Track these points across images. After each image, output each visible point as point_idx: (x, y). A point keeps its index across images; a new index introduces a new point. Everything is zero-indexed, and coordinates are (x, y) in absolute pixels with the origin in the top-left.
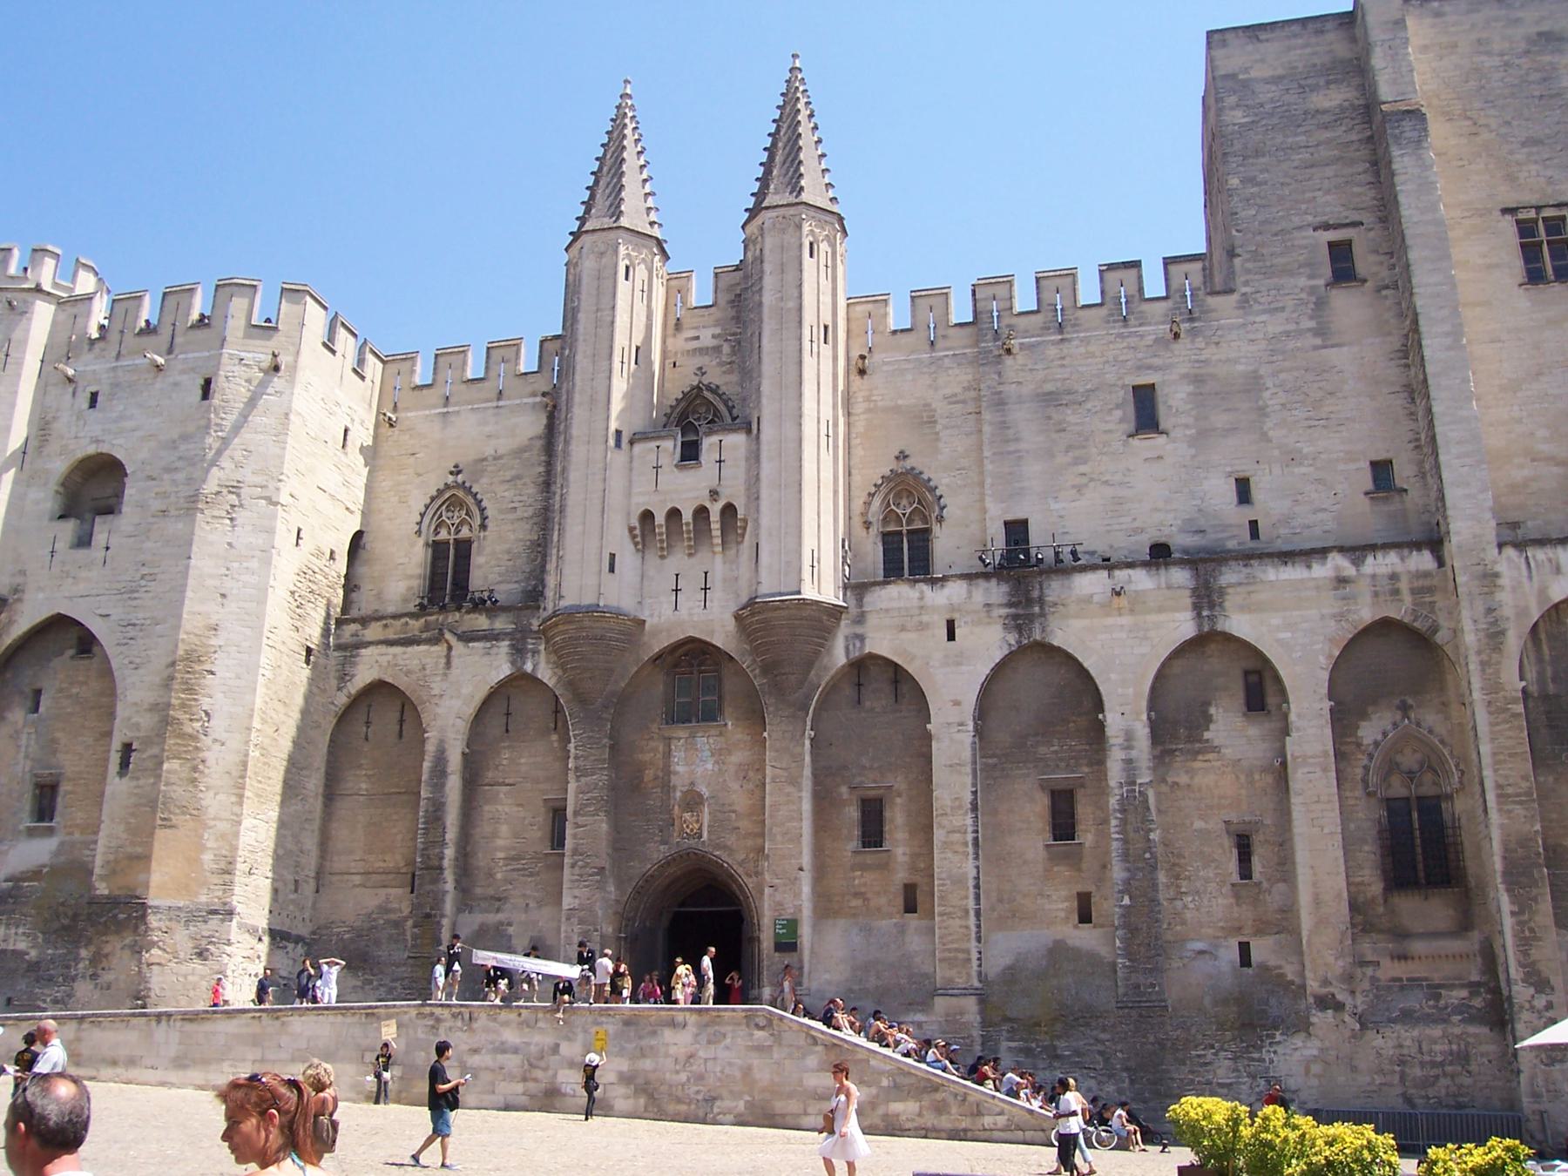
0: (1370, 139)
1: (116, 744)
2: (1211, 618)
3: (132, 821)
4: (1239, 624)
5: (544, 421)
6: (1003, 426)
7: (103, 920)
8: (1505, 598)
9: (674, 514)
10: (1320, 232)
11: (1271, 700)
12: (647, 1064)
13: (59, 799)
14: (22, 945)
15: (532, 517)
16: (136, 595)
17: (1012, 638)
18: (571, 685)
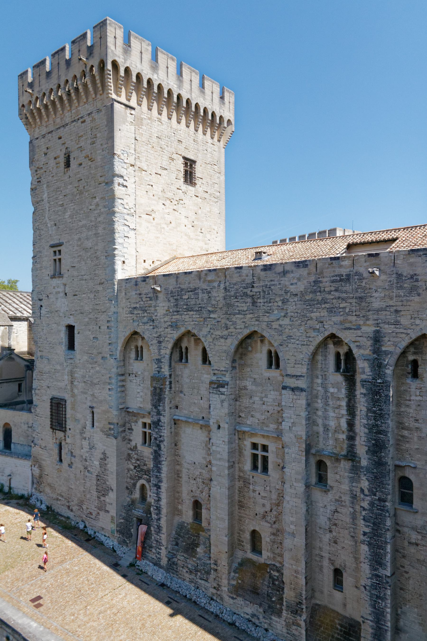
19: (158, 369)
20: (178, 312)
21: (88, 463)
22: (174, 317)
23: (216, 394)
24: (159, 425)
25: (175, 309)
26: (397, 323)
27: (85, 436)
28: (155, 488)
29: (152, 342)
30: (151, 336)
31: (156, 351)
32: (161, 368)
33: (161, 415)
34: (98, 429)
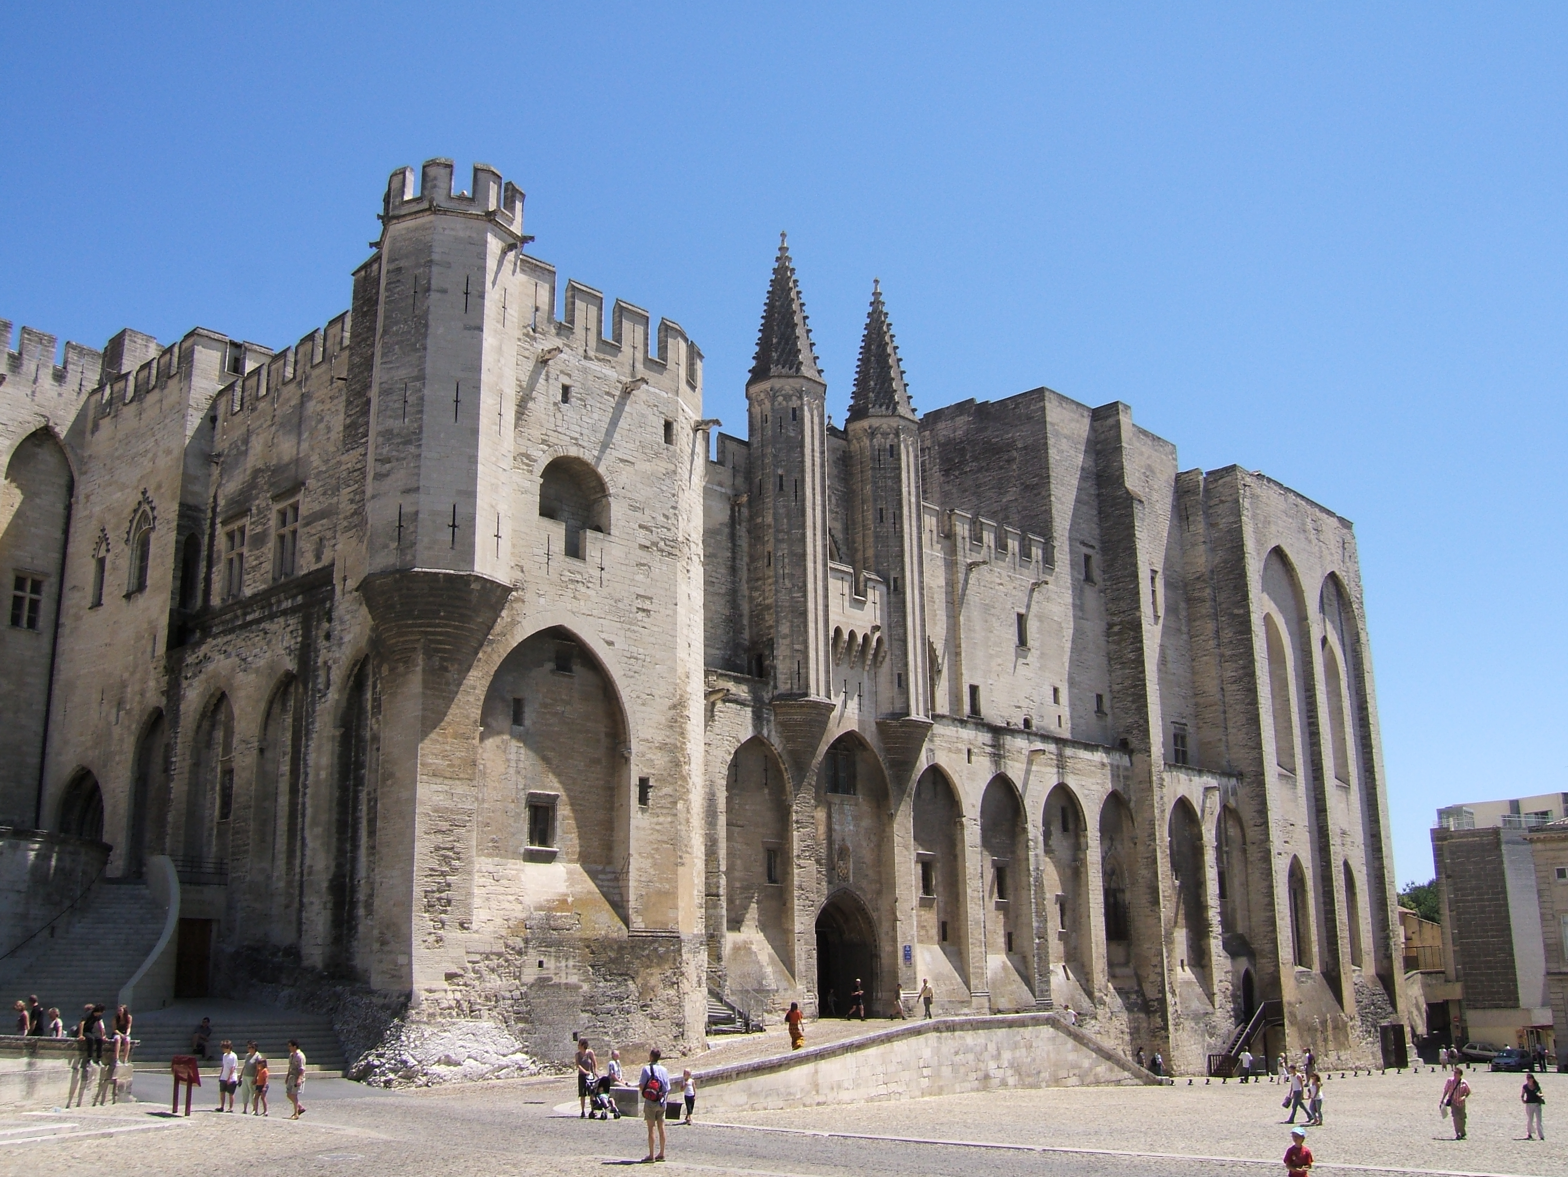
0: (1098, 495)
1: (634, 781)
2: (1063, 774)
3: (657, 856)
4: (1072, 783)
5: (729, 512)
6: (969, 619)
7: (647, 952)
8: (1164, 790)
9: (852, 634)
10: (1081, 547)
11: (1071, 826)
12: (1017, 1053)
13: (558, 824)
14: (574, 979)
15: (724, 595)
16: (633, 628)
17: (993, 768)
18: (791, 753)
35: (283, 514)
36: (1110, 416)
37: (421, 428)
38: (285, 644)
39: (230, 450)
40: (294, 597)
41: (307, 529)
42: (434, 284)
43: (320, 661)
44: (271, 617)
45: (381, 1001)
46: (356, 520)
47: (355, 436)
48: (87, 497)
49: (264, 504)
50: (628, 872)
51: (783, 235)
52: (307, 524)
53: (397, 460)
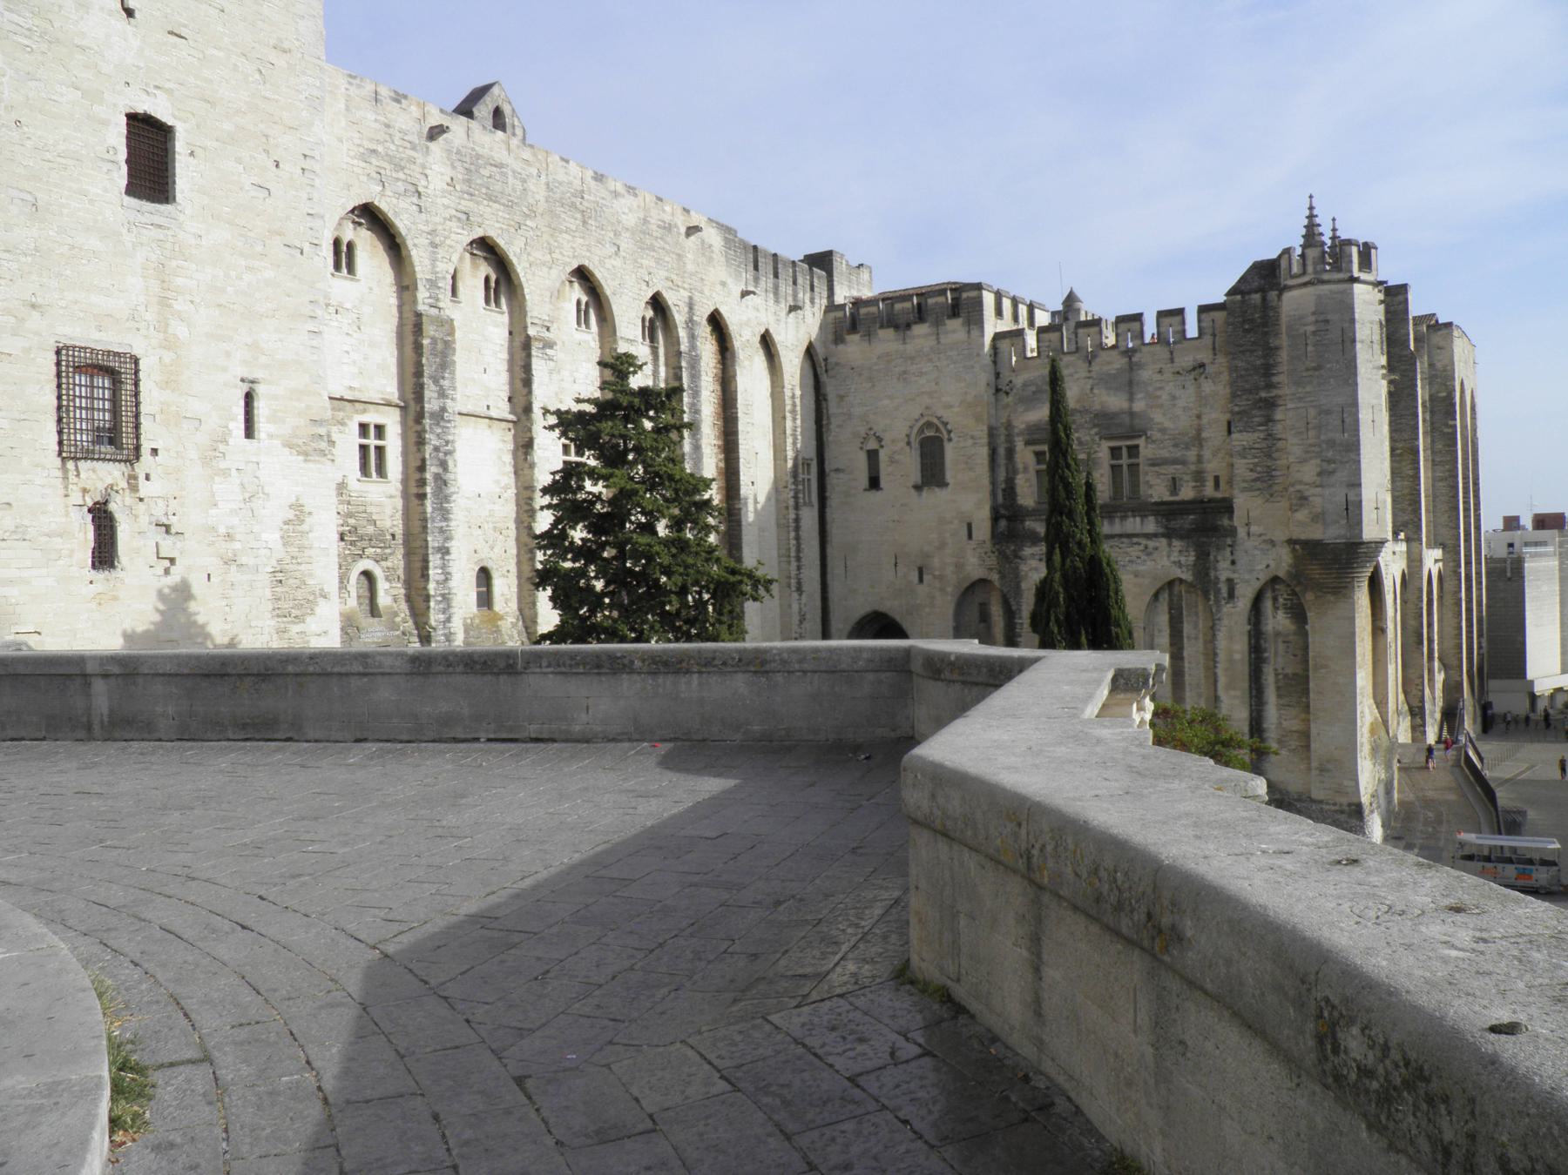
19: (430, 301)
20: (472, 195)
21: (237, 545)
22: (463, 202)
23: (542, 358)
24: (442, 418)
25: (465, 188)
26: (701, 292)
27: (223, 465)
28: (439, 556)
29: (416, 241)
30: (413, 227)
31: (427, 262)
32: (438, 300)
33: (447, 397)
34: (277, 442)
35: (1115, 452)
36: (1399, 294)
37: (1358, 441)
38: (1172, 559)
39: (1025, 385)
40: (1143, 517)
41: (1157, 469)
42: (1359, 336)
43: (1223, 578)
44: (1148, 536)
45: (1334, 808)
46: (1258, 484)
47: (1247, 422)
48: (841, 398)
49: (1088, 438)
50: (1387, 703)
51: (1311, 197)
52: (1153, 465)
53: (1341, 462)
